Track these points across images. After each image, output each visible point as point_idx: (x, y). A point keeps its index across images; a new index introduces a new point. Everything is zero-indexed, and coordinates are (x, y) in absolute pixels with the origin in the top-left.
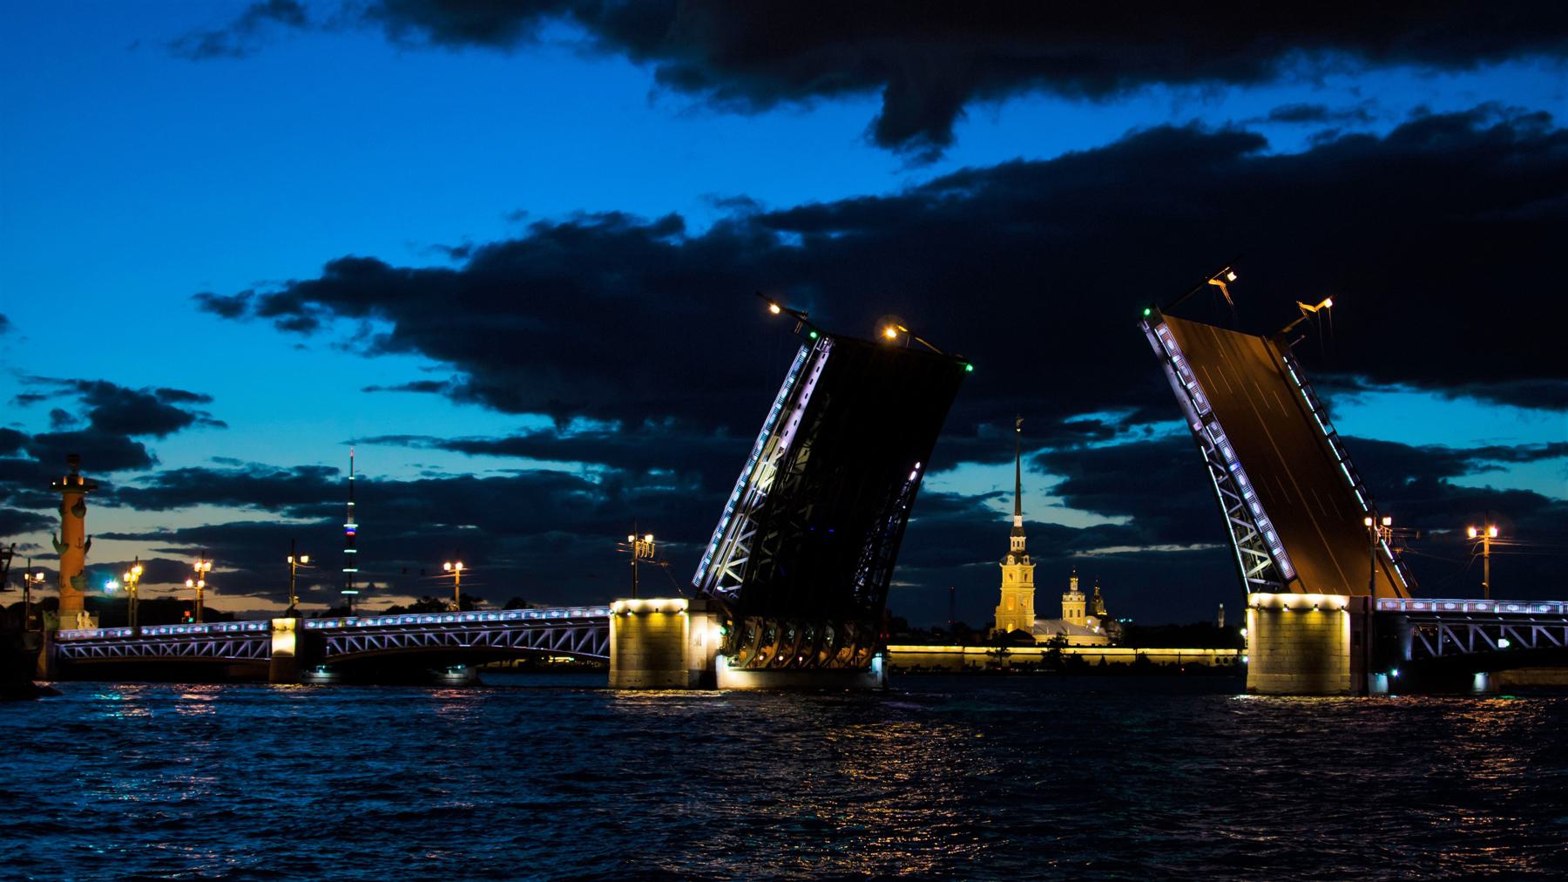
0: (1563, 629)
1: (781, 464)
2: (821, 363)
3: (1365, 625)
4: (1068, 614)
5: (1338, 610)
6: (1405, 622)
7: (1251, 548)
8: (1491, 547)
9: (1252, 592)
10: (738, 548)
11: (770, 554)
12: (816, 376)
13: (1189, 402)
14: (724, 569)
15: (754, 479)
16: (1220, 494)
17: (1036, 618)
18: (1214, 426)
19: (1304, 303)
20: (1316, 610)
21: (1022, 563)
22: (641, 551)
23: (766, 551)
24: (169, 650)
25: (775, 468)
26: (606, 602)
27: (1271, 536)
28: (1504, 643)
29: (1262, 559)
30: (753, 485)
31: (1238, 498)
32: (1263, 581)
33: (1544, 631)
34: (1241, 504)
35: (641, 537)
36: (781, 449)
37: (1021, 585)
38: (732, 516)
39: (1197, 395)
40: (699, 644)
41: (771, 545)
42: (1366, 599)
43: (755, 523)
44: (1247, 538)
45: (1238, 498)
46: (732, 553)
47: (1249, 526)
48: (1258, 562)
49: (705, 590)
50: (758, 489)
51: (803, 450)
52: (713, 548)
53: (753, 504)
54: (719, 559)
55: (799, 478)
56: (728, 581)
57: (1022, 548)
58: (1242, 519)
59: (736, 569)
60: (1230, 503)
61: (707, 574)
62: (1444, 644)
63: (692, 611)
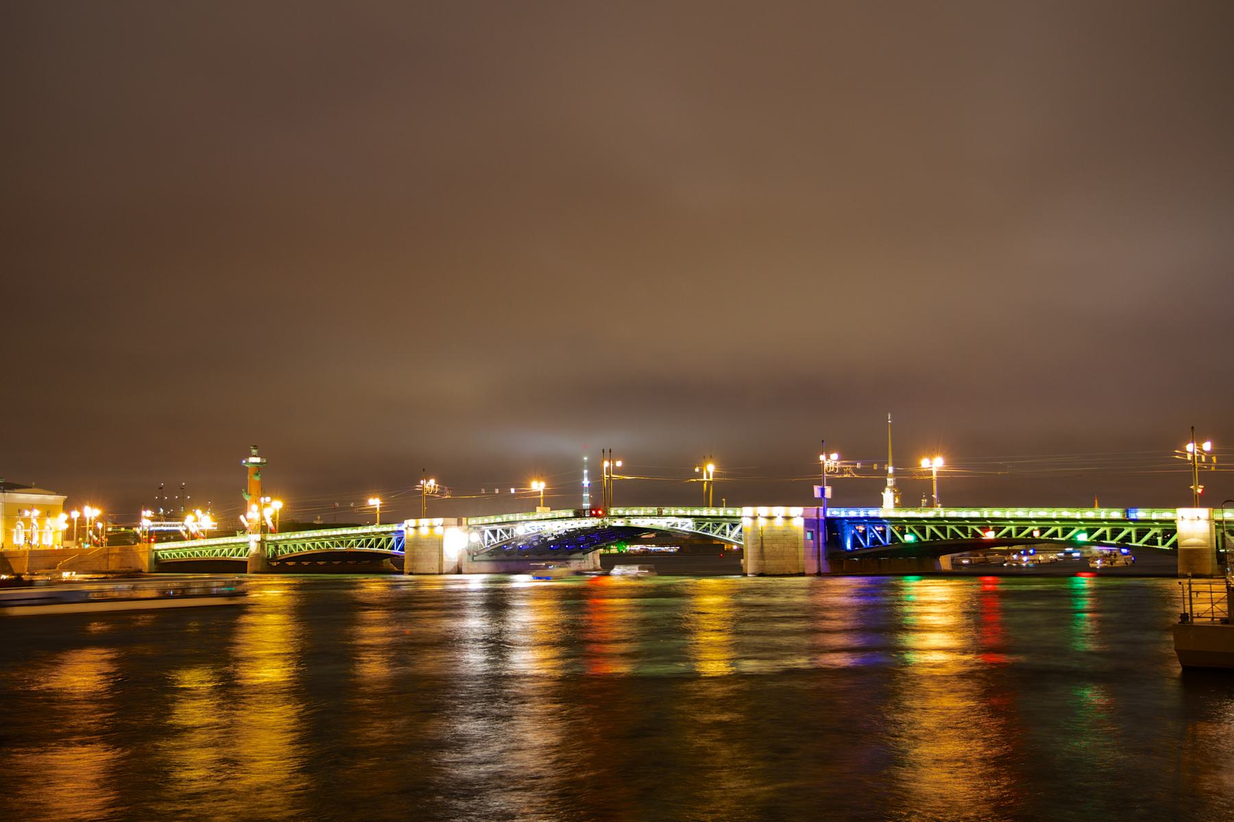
0: (946, 528)
24: (207, 554)
26: (401, 522)
28: (909, 538)
35: (427, 481)
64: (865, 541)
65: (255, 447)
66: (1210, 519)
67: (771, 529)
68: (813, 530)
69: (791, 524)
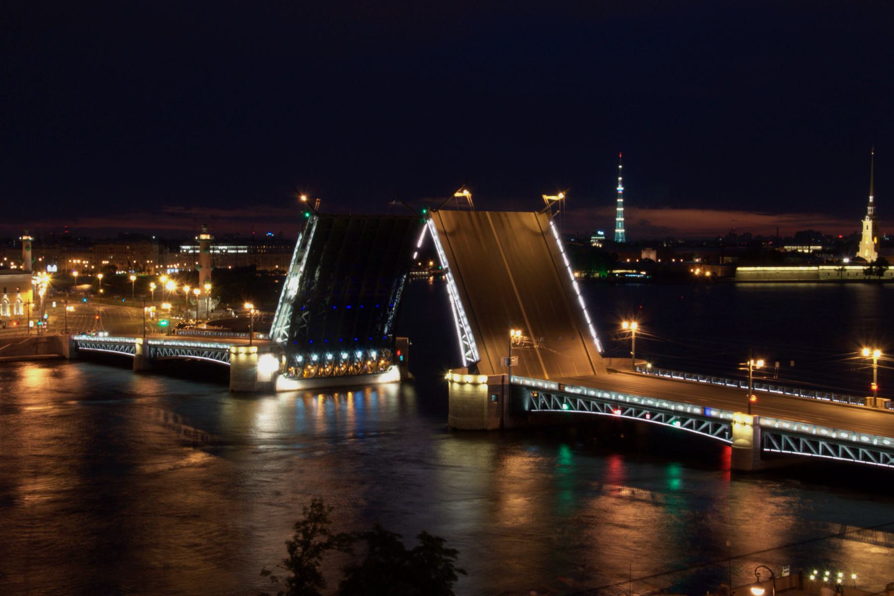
2: (314, 229)
3: (503, 391)
8: (636, 334)
12: (312, 235)
19: (548, 195)
33: (582, 402)
38: (282, 304)
46: (285, 322)
51: (317, 271)
55: (316, 285)
56: (284, 336)
63: (259, 353)
65: (205, 226)
66: (755, 425)
67: (462, 392)
69: (478, 390)
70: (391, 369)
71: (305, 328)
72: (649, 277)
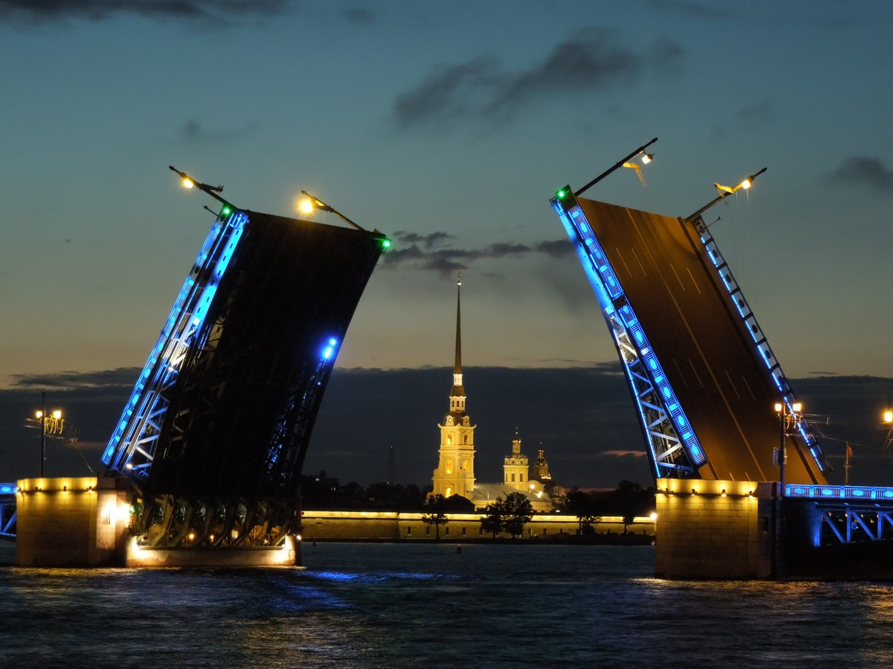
1: (194, 342)
2: (235, 239)
4: (509, 478)
5: (746, 496)
6: (813, 508)
7: (662, 432)
9: (662, 477)
10: (148, 425)
11: (181, 430)
13: (601, 286)
14: (136, 446)
15: (166, 355)
16: (631, 378)
17: (476, 482)
18: (626, 309)
19: (721, 185)
20: (724, 495)
21: (462, 425)
22: (50, 427)
23: (177, 428)
25: (187, 345)
27: (681, 421)
29: (673, 444)
30: (165, 361)
31: (649, 382)
32: (673, 466)
34: (652, 388)
36: (193, 326)
37: (461, 447)
39: (610, 278)
40: (107, 522)
41: (182, 422)
42: (775, 485)
43: (165, 400)
44: (658, 422)
45: (649, 382)
47: (660, 410)
48: (669, 446)
49: (115, 468)
50: (170, 365)
51: (216, 327)
52: (123, 425)
53: (165, 381)
54: (129, 435)
55: (212, 354)
56: (138, 458)
57: (462, 408)
58: (653, 403)
59: (146, 447)
60: (641, 386)
61: (116, 451)
62: (853, 531)
63: (100, 489)
64: (843, 532)
67: (711, 512)
68: (768, 515)
69: (739, 507)
70: (283, 542)
71: (180, 443)
72: (283, 476)
